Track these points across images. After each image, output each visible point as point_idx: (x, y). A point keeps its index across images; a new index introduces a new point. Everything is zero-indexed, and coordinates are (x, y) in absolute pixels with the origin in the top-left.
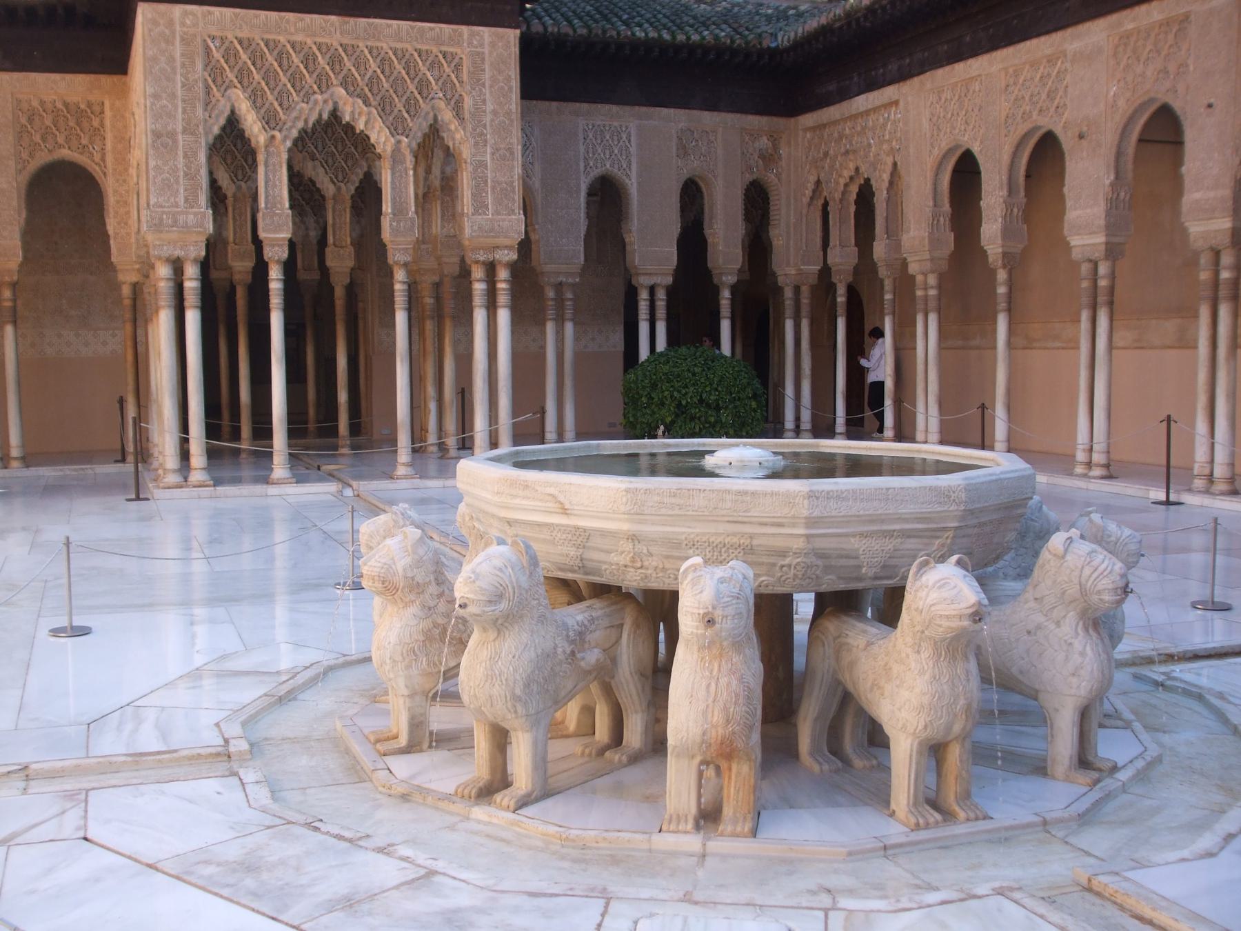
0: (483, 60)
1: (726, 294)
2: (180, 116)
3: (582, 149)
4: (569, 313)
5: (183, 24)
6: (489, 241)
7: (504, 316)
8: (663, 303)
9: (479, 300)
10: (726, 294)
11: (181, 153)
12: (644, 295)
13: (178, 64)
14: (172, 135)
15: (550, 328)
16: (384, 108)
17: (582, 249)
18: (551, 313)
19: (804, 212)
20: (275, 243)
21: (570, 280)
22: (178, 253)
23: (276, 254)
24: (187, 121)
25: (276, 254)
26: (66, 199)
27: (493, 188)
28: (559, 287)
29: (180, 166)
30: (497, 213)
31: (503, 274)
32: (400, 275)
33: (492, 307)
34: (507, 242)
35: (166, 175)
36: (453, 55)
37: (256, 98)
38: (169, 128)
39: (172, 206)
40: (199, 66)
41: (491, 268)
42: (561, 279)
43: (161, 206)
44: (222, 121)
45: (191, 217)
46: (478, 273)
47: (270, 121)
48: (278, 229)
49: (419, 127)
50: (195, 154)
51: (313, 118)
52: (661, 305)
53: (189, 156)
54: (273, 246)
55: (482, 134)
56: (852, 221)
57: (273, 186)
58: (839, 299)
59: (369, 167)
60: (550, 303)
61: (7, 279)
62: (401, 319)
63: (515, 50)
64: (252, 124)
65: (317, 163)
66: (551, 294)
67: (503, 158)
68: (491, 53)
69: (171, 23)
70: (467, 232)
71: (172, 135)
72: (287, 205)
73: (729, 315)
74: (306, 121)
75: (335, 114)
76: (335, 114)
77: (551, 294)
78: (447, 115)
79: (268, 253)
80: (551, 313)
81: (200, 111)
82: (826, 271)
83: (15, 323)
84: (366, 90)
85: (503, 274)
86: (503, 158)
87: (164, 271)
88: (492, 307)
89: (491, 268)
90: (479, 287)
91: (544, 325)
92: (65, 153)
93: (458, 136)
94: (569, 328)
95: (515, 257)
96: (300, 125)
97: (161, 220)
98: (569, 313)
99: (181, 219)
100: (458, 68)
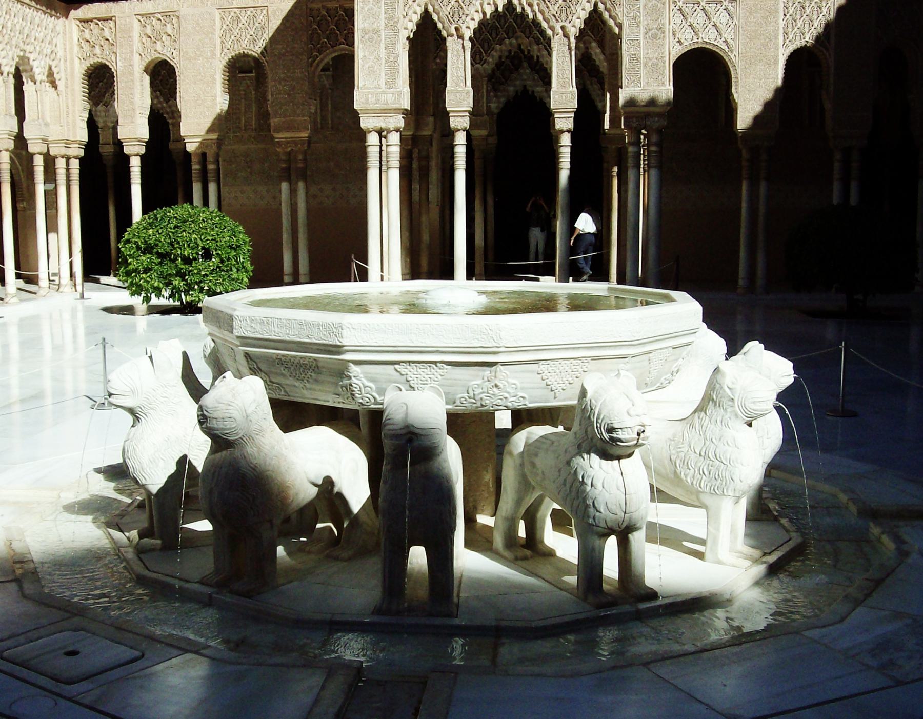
2: (383, 16)
3: (782, 23)
11: (383, 46)
14: (376, 32)
22: (383, 126)
23: (460, 122)
24: (389, 19)
25: (460, 122)
27: (645, 65)
35: (371, 63)
38: (375, 26)
51: (489, 10)
53: (391, 47)
59: (587, 48)
67: (655, 37)
71: (376, 32)
77: (745, 154)
83: (305, 180)
86: (655, 37)
91: (741, 182)
96: (478, 17)
99: (382, 98)
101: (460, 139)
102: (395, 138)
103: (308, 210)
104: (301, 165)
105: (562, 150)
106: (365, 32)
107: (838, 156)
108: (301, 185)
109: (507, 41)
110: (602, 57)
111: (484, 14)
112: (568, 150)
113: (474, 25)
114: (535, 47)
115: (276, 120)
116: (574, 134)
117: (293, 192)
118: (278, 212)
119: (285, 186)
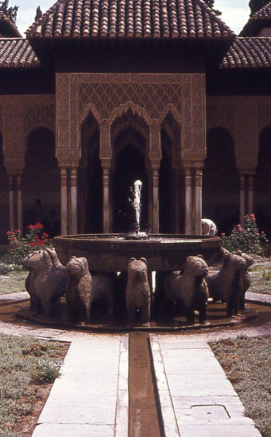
0: (190, 87)
5: (72, 80)
6: (192, 159)
7: (199, 191)
9: (188, 183)
11: (70, 127)
13: (69, 95)
14: (67, 121)
15: (242, 193)
16: (148, 108)
20: (105, 161)
26: (41, 141)
28: (247, 176)
29: (69, 133)
36: (177, 85)
37: (99, 106)
39: (66, 148)
40: (77, 95)
43: (62, 148)
44: (85, 115)
45: (73, 151)
47: (104, 115)
49: (163, 114)
50: (75, 128)
53: (73, 128)
55: (189, 116)
57: (106, 140)
60: (251, 183)
61: (19, 173)
63: (204, 82)
64: (96, 114)
65: (141, 126)
68: (193, 84)
69: (67, 80)
70: (182, 155)
72: (110, 146)
74: (118, 114)
75: (130, 110)
76: (130, 110)
78: (174, 109)
81: (77, 112)
84: (142, 101)
87: (64, 172)
92: (42, 124)
93: (179, 117)
94: (251, 193)
95: (203, 165)
97: (62, 153)
98: (251, 187)
100: (179, 91)
101: (106, 172)
102: (74, 171)
103: (23, 206)
104: (19, 183)
105: (154, 178)
106: (60, 120)
108: (19, 192)
109: (124, 123)
110: (171, 131)
111: (118, 114)
112: (157, 178)
113: (113, 119)
114: (138, 126)
115: (8, 159)
116: (161, 171)
117: (15, 198)
118: (8, 206)
119: (11, 193)
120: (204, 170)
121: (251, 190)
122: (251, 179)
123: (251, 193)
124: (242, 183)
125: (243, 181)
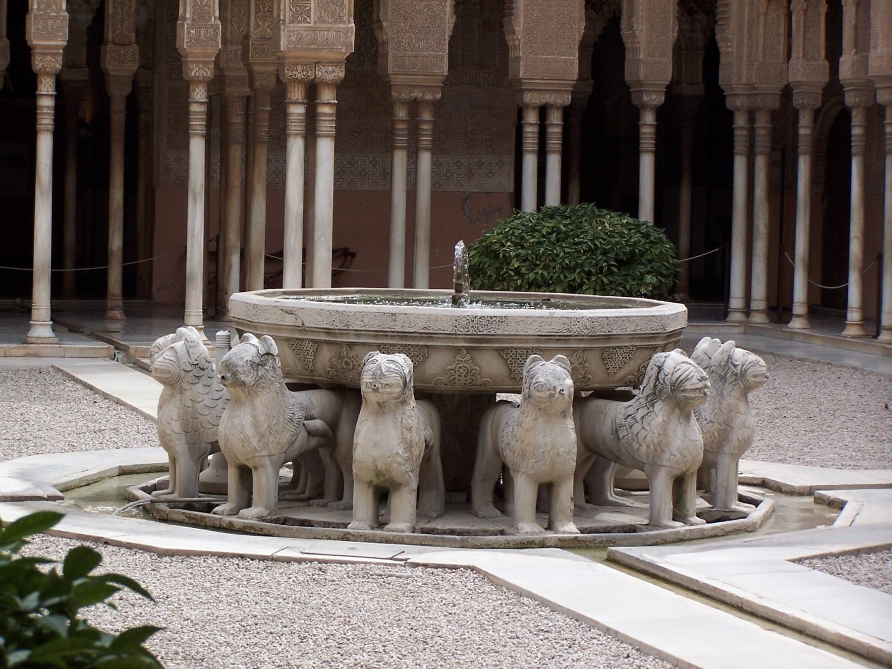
1: (649, 118)
4: (426, 140)
6: (311, 54)
7: (326, 149)
8: (558, 130)
10: (649, 118)
12: (532, 117)
15: (400, 159)
17: (446, 56)
18: (402, 139)
19: (762, 9)
20: (48, 51)
21: (429, 97)
28: (414, 106)
30: (321, 19)
31: (328, 96)
32: (199, 94)
33: (311, 137)
34: (333, 56)
41: (312, 90)
42: (417, 94)
46: (297, 94)
48: (51, 35)
52: (555, 131)
54: (44, 54)
56: (823, 26)
58: (802, 131)
62: (197, 149)
66: (402, 114)
72: (64, 7)
73: (652, 148)
77: (402, 114)
79: (38, 63)
80: (402, 139)
82: (787, 92)
85: (328, 96)
88: (311, 137)
89: (312, 90)
90: (297, 111)
94: (425, 160)
95: (342, 75)
98: (426, 140)
101: (46, 88)
105: (194, 108)
107: (532, 117)
120: (340, 87)
121: (427, 149)
122: (427, 116)
123: (425, 160)
124: (401, 126)
125: (403, 121)
